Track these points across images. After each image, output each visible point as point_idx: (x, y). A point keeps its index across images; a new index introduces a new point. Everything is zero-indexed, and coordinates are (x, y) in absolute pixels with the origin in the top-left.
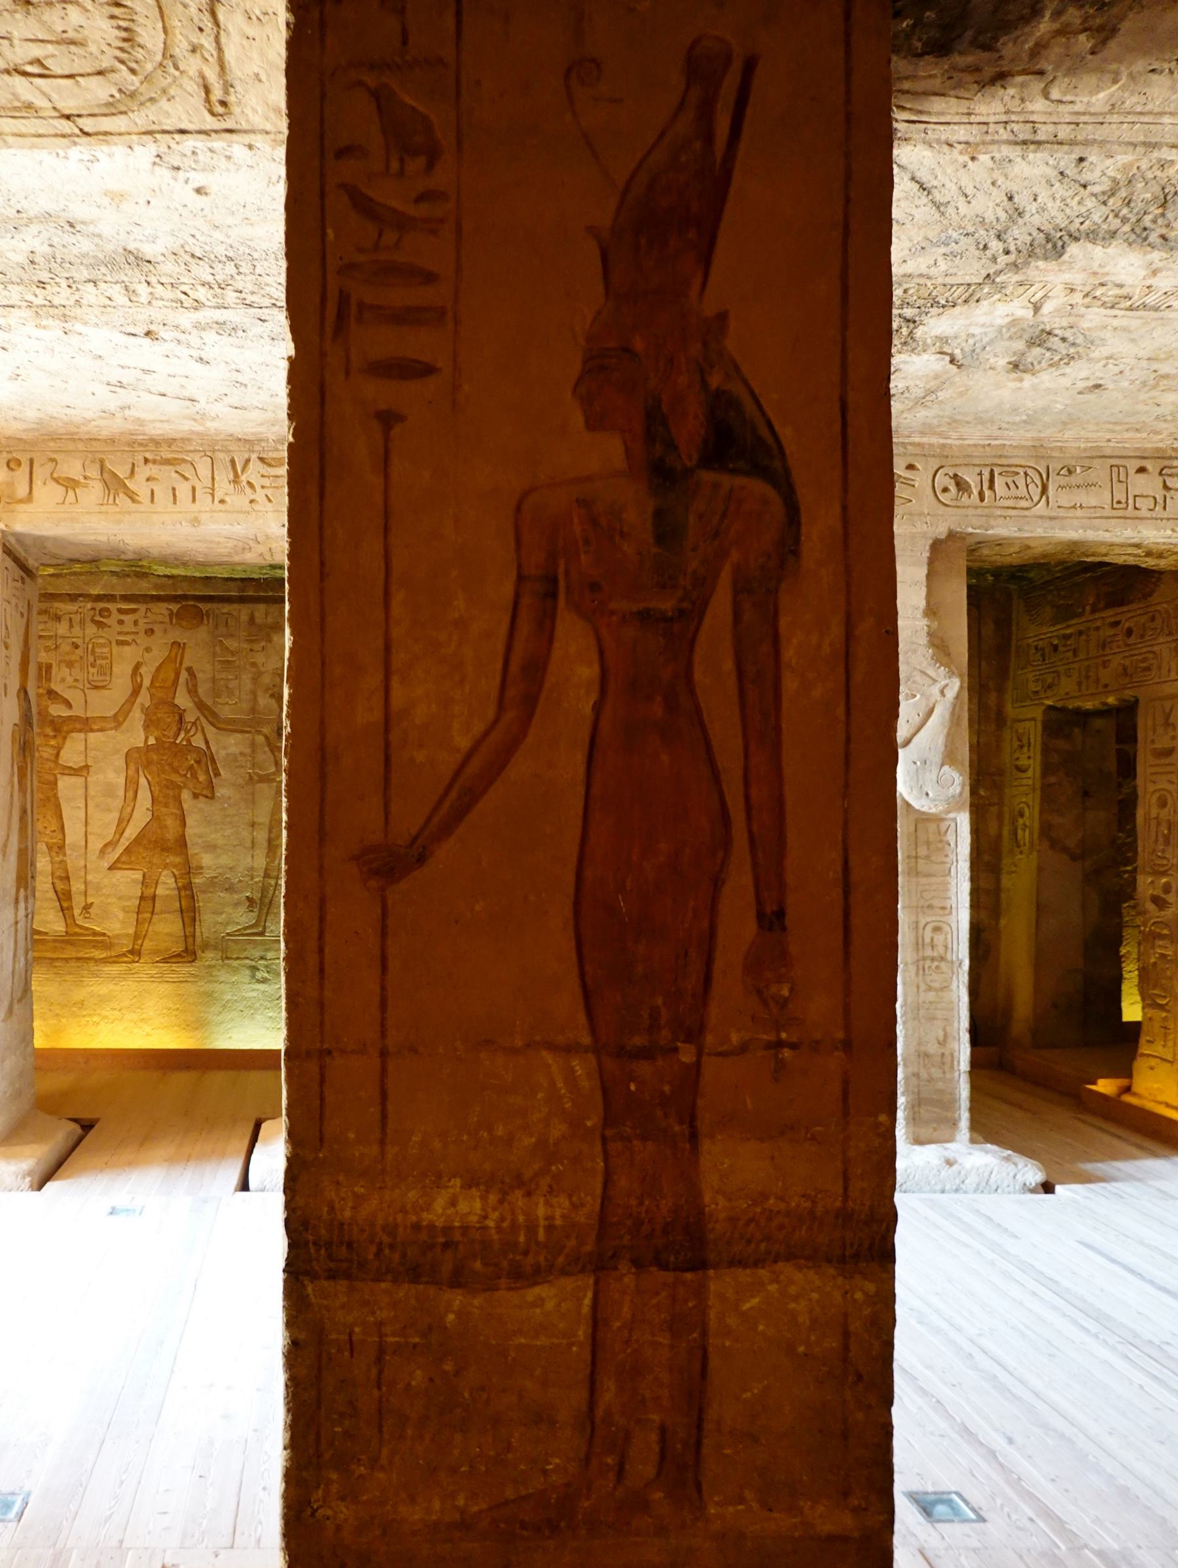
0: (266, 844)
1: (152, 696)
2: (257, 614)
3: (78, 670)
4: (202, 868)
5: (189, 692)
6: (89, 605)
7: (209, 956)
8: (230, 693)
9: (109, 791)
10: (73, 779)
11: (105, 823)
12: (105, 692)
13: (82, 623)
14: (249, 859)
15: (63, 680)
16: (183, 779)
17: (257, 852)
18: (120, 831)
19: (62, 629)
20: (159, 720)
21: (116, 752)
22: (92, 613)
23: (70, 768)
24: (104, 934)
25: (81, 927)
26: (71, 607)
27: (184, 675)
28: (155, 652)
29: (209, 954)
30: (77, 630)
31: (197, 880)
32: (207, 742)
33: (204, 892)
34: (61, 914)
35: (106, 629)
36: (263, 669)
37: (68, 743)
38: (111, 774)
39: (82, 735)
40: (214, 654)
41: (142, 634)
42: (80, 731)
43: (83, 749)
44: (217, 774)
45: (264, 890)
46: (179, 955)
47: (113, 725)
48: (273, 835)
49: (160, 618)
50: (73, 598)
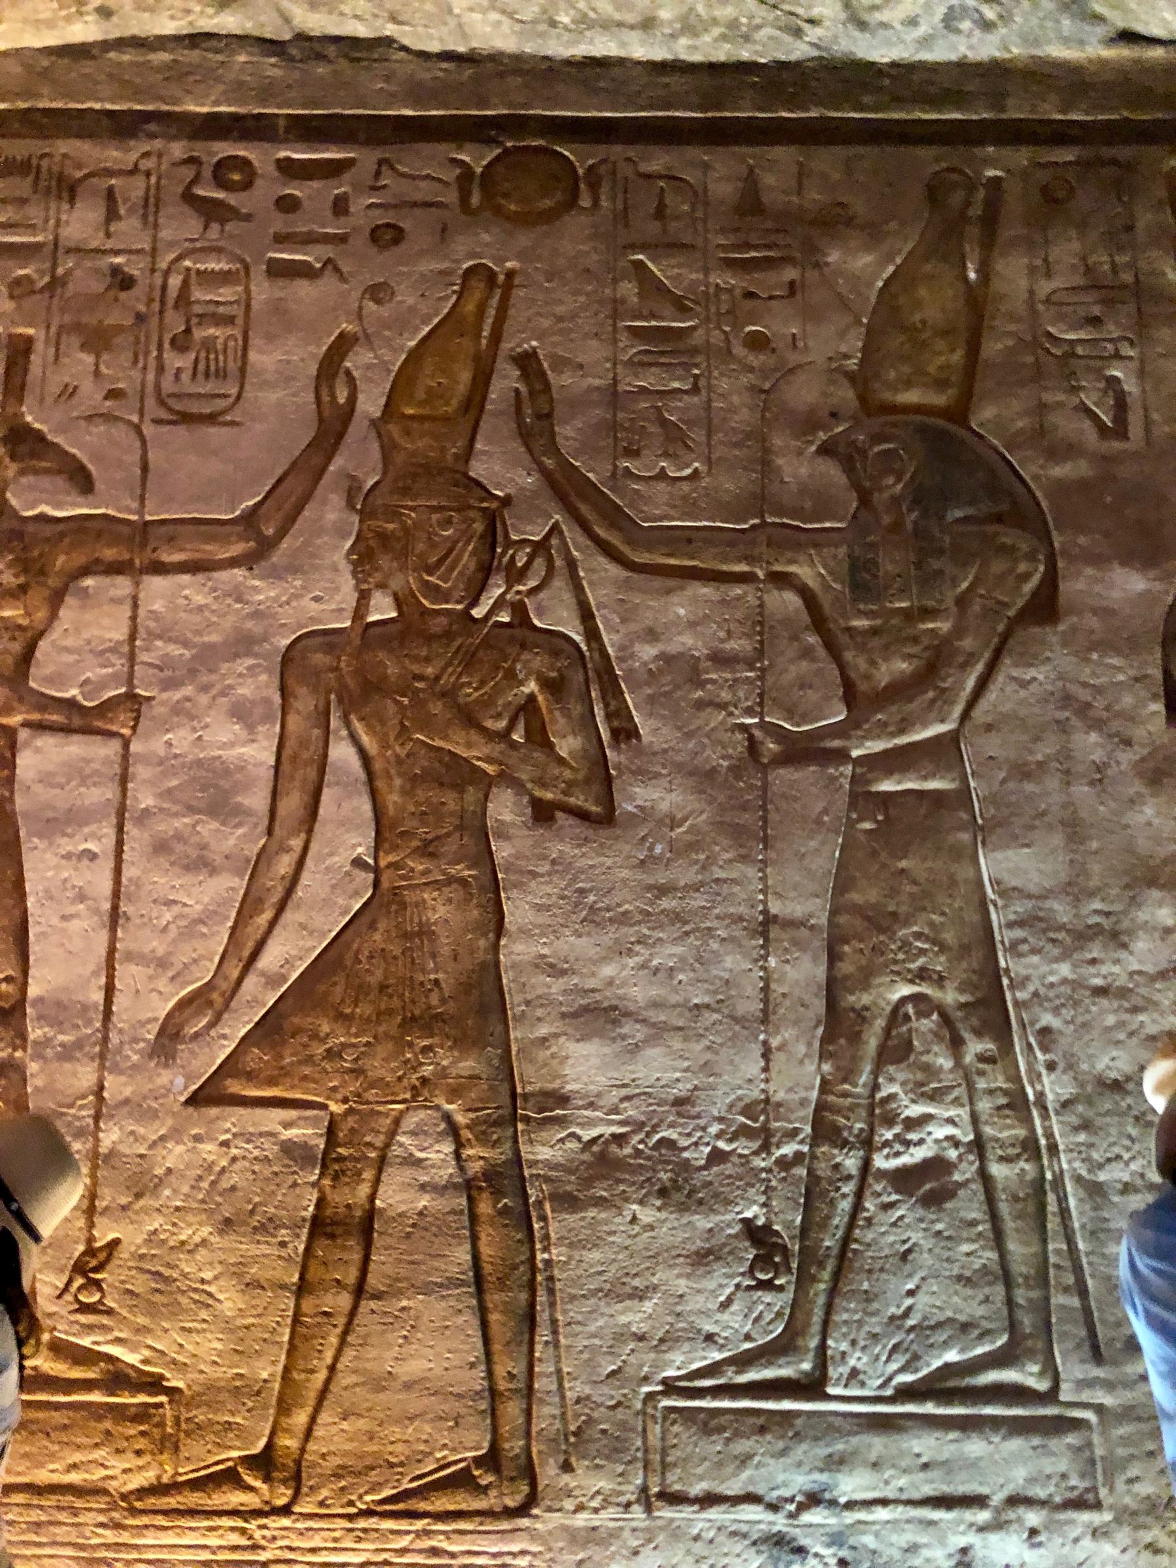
0: (819, 1006)
2: (769, 179)
3: (125, 358)
4: (563, 1100)
5: (525, 435)
6: (178, 149)
7: (589, 1493)
8: (674, 439)
9: (213, 791)
10: (76, 748)
11: (189, 905)
12: (215, 434)
13: (150, 207)
14: (753, 1066)
15: (69, 392)
16: (496, 749)
17: (788, 1034)
18: (245, 952)
19: (80, 223)
21: (243, 644)
22: (188, 173)
23: (72, 703)
24: (154, 1384)
26: (114, 155)
27: (506, 381)
28: (406, 297)
29: (590, 1481)
30: (129, 228)
31: (544, 1150)
32: (586, 616)
33: (568, 1202)
36: (793, 359)
37: (66, 613)
39: (122, 585)
40: (617, 309)
41: (360, 242)
43: (120, 634)
44: (625, 732)
45: (815, 1195)
46: (462, 1481)
47: (237, 549)
48: (846, 968)
49: (423, 191)
50: (123, 126)
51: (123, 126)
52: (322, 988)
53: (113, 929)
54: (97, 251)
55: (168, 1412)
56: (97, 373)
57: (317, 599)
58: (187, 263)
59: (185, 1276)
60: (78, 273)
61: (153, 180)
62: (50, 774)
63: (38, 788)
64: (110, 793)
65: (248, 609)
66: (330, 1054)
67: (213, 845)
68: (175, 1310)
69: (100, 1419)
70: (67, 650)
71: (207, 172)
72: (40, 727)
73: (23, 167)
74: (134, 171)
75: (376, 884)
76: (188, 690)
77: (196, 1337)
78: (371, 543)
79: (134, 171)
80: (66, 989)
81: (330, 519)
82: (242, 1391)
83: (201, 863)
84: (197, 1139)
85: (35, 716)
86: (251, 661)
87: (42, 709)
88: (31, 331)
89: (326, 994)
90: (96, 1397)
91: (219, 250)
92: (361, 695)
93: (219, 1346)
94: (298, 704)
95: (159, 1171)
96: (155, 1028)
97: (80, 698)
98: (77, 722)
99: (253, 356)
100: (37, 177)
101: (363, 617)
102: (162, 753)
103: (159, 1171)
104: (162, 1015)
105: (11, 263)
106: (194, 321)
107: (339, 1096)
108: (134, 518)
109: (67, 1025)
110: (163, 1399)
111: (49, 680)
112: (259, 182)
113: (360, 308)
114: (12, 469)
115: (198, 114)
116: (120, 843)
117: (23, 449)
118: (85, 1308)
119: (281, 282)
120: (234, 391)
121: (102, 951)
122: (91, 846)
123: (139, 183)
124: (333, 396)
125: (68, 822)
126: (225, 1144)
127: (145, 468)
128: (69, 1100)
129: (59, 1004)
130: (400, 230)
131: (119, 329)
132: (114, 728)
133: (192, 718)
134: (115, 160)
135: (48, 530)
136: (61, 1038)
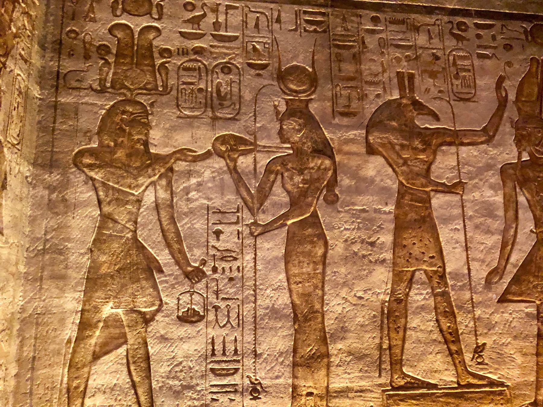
1: (519, 109)
6: (446, 19)
9: (488, 210)
10: (448, 198)
13: (441, 35)
15: (427, 91)
18: (505, 257)
19: (422, 40)
20: (529, 135)
22: (450, 26)
23: (444, 184)
24: (502, 384)
25: (474, 376)
26: (428, 19)
34: (450, 359)
35: (465, 42)
37: (439, 158)
38: (489, 193)
39: (453, 149)
41: (501, 49)
42: (450, 144)
43: (455, 164)
47: (483, 139)
50: (429, 11)
51: (429, 11)
52: (528, 268)
53: (467, 251)
54: (426, 48)
55: (507, 392)
56: (435, 85)
57: (507, 154)
58: (454, 53)
59: (506, 352)
60: (423, 55)
61: (440, 28)
62: (442, 205)
63: (440, 210)
64: (460, 211)
65: (489, 156)
66: (535, 287)
67: (491, 226)
68: (505, 363)
69: (489, 395)
70: (441, 168)
71: (455, 26)
72: (436, 191)
73: (403, 22)
74: (434, 25)
75: (537, 237)
76: (476, 181)
77: (512, 370)
78: (520, 137)
79: (434, 25)
80: (457, 269)
81: (506, 130)
82: (526, 384)
83: (489, 232)
84: (503, 312)
85: (435, 188)
86: (492, 172)
87: (437, 186)
88: (413, 72)
89: (530, 269)
90: (487, 389)
91: (462, 49)
92: (524, 182)
93: (518, 372)
94: (508, 185)
95: (493, 323)
96: (484, 280)
97: (446, 183)
98: (446, 190)
99: (477, 82)
100: (407, 24)
101: (521, 159)
102: (472, 199)
103: (493, 323)
104: (485, 276)
105: (404, 51)
106: (459, 70)
107: (539, 299)
108: (453, 129)
109: (460, 280)
110: (505, 388)
111: (437, 177)
112: (470, 29)
113: (505, 68)
114: (415, 113)
115: (450, 8)
116: (465, 226)
117: (416, 107)
118: (479, 363)
119: (481, 60)
120: (473, 92)
121: (465, 257)
122: (457, 227)
123: (437, 28)
124: (501, 95)
125: (450, 220)
126: (510, 314)
127: (453, 114)
128: (464, 302)
129: (456, 274)
130: (511, 46)
131: (438, 72)
132: (458, 192)
133: (479, 189)
134: (429, 22)
135: (428, 132)
136: (459, 284)
